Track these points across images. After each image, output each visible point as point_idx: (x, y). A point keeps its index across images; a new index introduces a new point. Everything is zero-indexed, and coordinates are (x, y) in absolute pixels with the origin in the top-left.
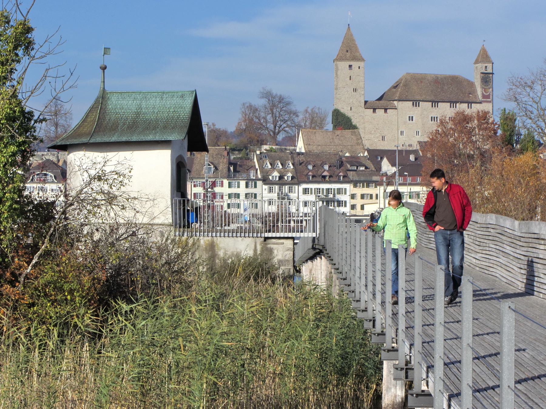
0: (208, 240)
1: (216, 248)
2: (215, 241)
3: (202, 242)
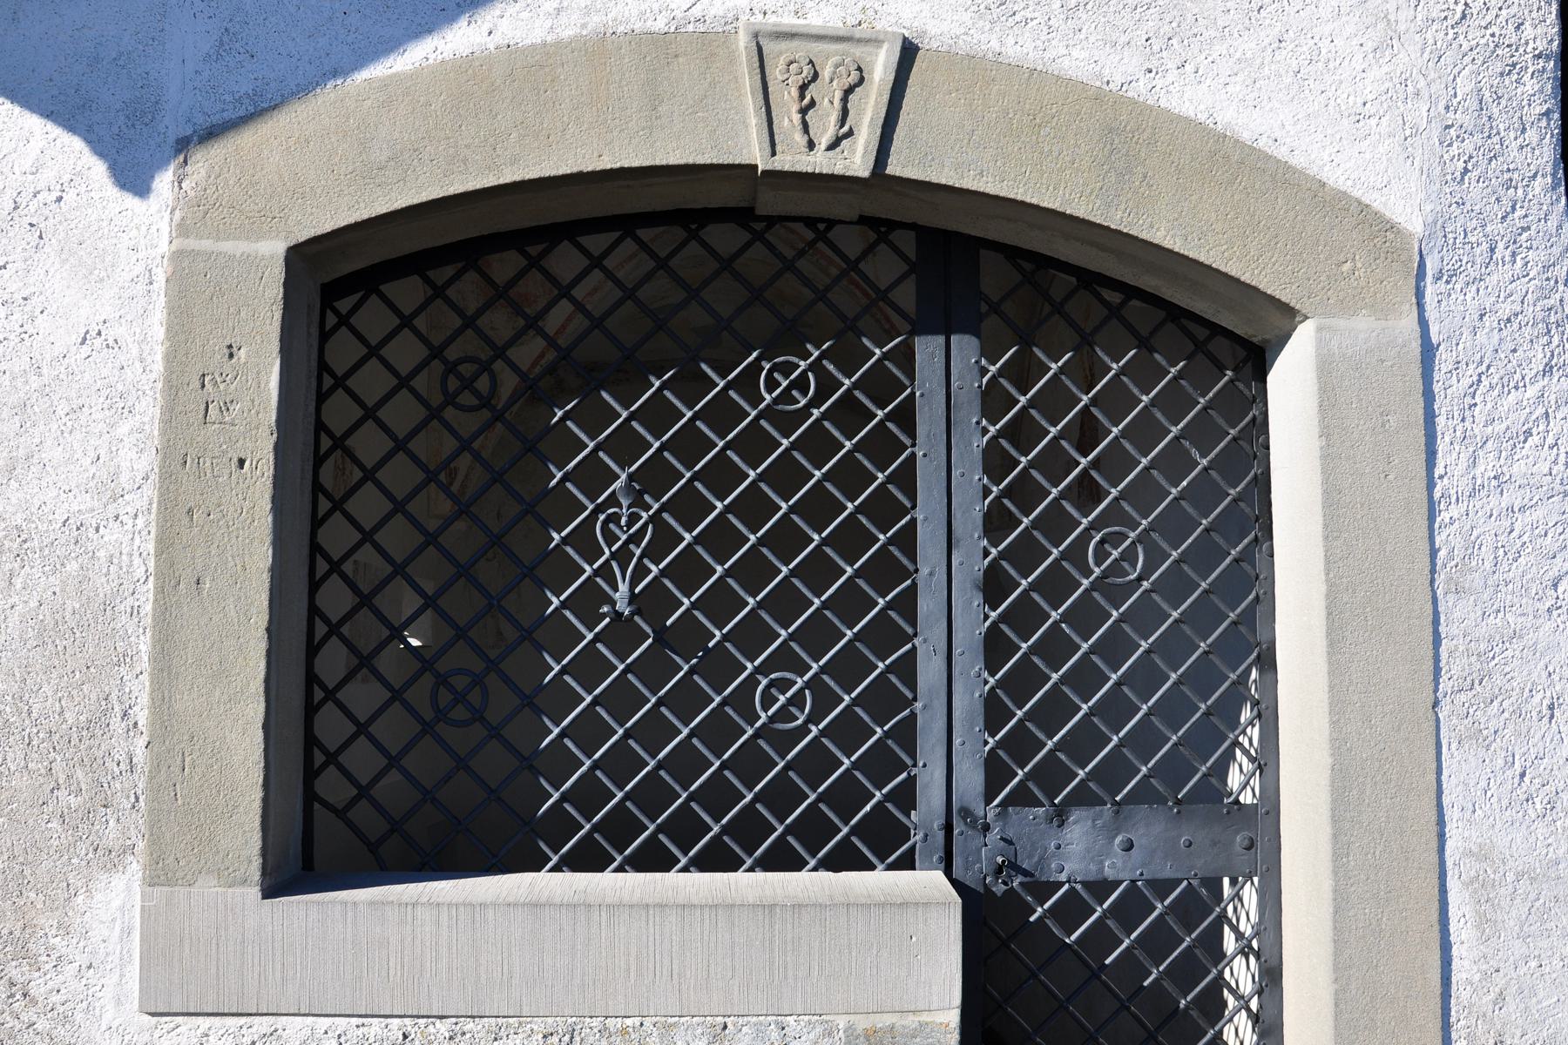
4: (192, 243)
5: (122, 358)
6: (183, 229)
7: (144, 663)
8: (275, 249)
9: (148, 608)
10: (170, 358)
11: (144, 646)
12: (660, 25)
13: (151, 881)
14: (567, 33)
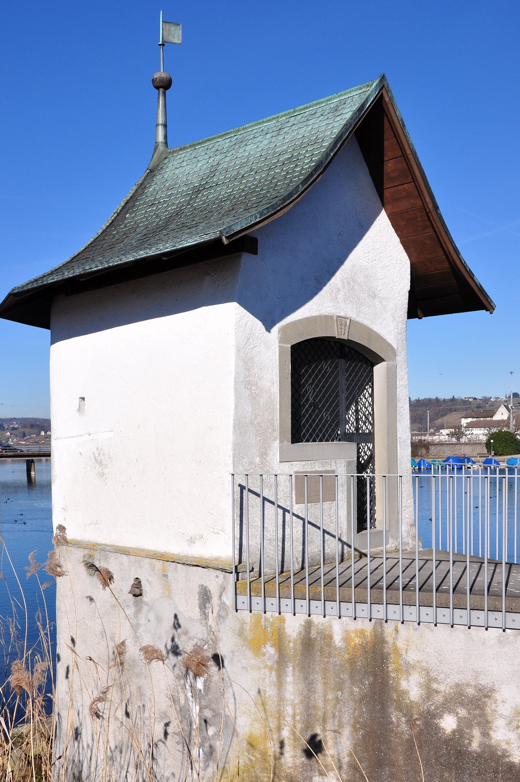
0: (362, 632)
1: (392, 667)
2: (389, 639)
3: (338, 639)
4: (282, 345)
5: (273, 362)
6: (280, 342)
7: (278, 409)
8: (289, 346)
9: (278, 401)
10: (279, 362)
11: (278, 407)
12: (327, 314)
13: (280, 442)
14: (318, 314)
